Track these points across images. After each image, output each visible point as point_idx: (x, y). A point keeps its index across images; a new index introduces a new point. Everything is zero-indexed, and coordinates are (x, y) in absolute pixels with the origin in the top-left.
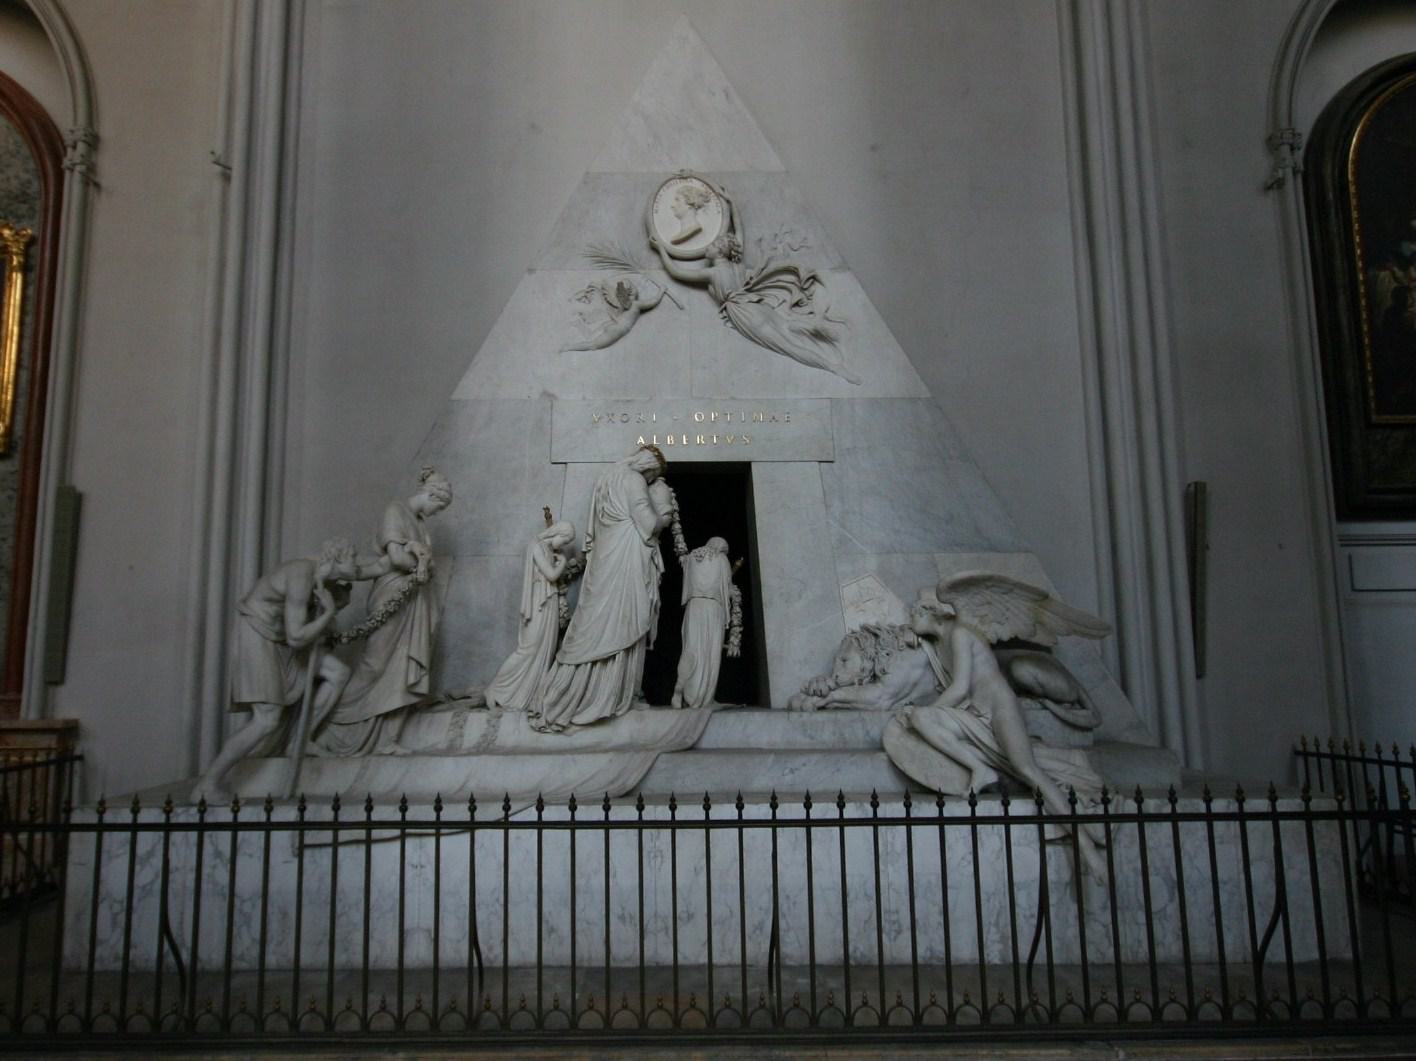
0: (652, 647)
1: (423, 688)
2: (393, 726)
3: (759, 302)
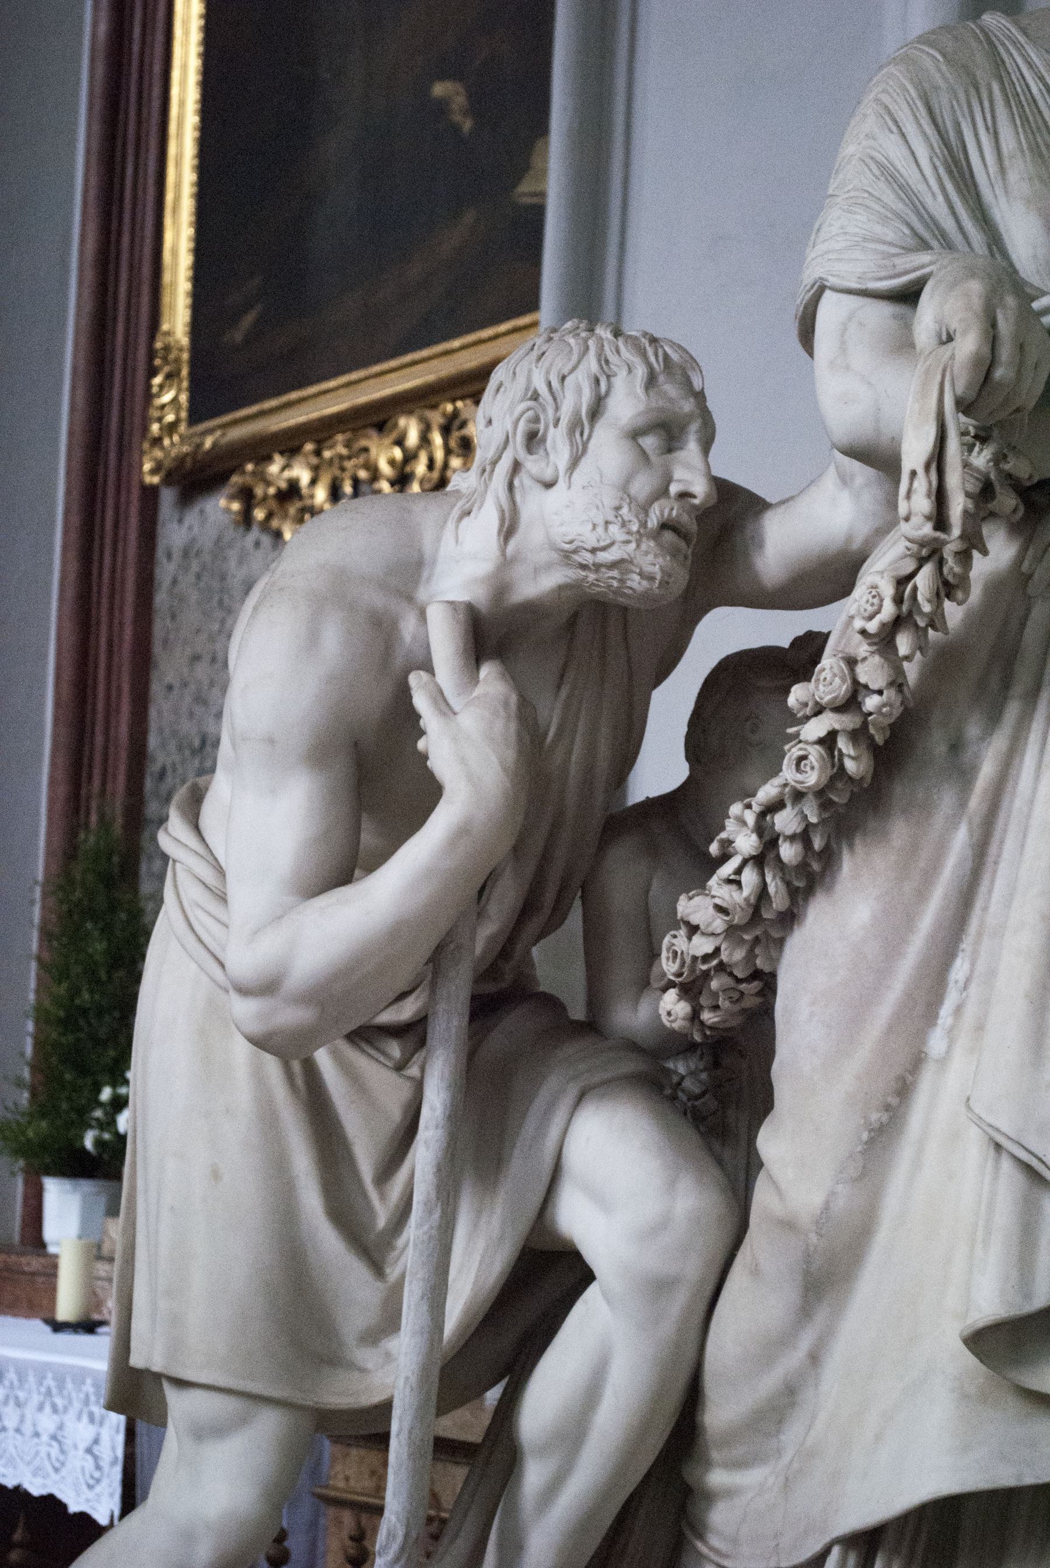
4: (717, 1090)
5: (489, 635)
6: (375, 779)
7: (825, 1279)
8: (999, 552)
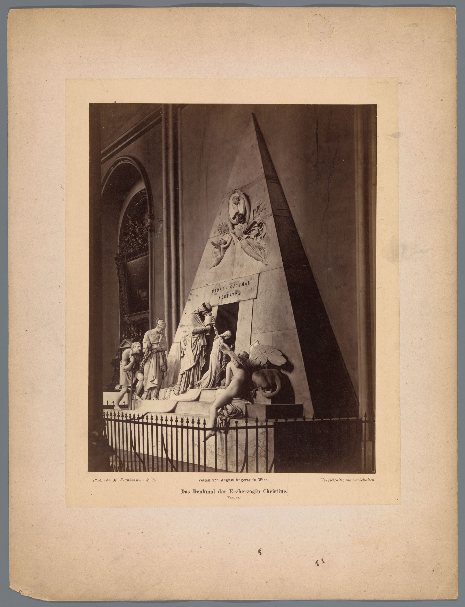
0: (201, 369)
1: (156, 381)
2: (154, 393)
3: (247, 238)
4: (142, 372)
5: (132, 355)
6: (128, 360)
7: (146, 380)
8: (150, 352)
